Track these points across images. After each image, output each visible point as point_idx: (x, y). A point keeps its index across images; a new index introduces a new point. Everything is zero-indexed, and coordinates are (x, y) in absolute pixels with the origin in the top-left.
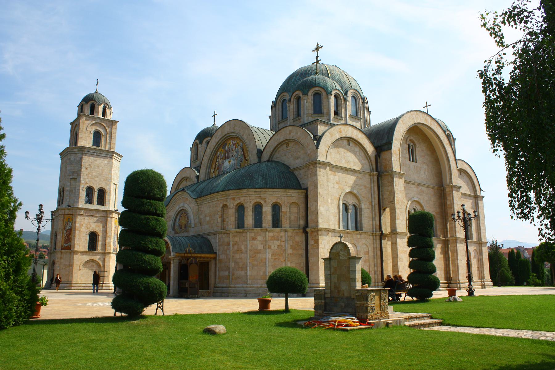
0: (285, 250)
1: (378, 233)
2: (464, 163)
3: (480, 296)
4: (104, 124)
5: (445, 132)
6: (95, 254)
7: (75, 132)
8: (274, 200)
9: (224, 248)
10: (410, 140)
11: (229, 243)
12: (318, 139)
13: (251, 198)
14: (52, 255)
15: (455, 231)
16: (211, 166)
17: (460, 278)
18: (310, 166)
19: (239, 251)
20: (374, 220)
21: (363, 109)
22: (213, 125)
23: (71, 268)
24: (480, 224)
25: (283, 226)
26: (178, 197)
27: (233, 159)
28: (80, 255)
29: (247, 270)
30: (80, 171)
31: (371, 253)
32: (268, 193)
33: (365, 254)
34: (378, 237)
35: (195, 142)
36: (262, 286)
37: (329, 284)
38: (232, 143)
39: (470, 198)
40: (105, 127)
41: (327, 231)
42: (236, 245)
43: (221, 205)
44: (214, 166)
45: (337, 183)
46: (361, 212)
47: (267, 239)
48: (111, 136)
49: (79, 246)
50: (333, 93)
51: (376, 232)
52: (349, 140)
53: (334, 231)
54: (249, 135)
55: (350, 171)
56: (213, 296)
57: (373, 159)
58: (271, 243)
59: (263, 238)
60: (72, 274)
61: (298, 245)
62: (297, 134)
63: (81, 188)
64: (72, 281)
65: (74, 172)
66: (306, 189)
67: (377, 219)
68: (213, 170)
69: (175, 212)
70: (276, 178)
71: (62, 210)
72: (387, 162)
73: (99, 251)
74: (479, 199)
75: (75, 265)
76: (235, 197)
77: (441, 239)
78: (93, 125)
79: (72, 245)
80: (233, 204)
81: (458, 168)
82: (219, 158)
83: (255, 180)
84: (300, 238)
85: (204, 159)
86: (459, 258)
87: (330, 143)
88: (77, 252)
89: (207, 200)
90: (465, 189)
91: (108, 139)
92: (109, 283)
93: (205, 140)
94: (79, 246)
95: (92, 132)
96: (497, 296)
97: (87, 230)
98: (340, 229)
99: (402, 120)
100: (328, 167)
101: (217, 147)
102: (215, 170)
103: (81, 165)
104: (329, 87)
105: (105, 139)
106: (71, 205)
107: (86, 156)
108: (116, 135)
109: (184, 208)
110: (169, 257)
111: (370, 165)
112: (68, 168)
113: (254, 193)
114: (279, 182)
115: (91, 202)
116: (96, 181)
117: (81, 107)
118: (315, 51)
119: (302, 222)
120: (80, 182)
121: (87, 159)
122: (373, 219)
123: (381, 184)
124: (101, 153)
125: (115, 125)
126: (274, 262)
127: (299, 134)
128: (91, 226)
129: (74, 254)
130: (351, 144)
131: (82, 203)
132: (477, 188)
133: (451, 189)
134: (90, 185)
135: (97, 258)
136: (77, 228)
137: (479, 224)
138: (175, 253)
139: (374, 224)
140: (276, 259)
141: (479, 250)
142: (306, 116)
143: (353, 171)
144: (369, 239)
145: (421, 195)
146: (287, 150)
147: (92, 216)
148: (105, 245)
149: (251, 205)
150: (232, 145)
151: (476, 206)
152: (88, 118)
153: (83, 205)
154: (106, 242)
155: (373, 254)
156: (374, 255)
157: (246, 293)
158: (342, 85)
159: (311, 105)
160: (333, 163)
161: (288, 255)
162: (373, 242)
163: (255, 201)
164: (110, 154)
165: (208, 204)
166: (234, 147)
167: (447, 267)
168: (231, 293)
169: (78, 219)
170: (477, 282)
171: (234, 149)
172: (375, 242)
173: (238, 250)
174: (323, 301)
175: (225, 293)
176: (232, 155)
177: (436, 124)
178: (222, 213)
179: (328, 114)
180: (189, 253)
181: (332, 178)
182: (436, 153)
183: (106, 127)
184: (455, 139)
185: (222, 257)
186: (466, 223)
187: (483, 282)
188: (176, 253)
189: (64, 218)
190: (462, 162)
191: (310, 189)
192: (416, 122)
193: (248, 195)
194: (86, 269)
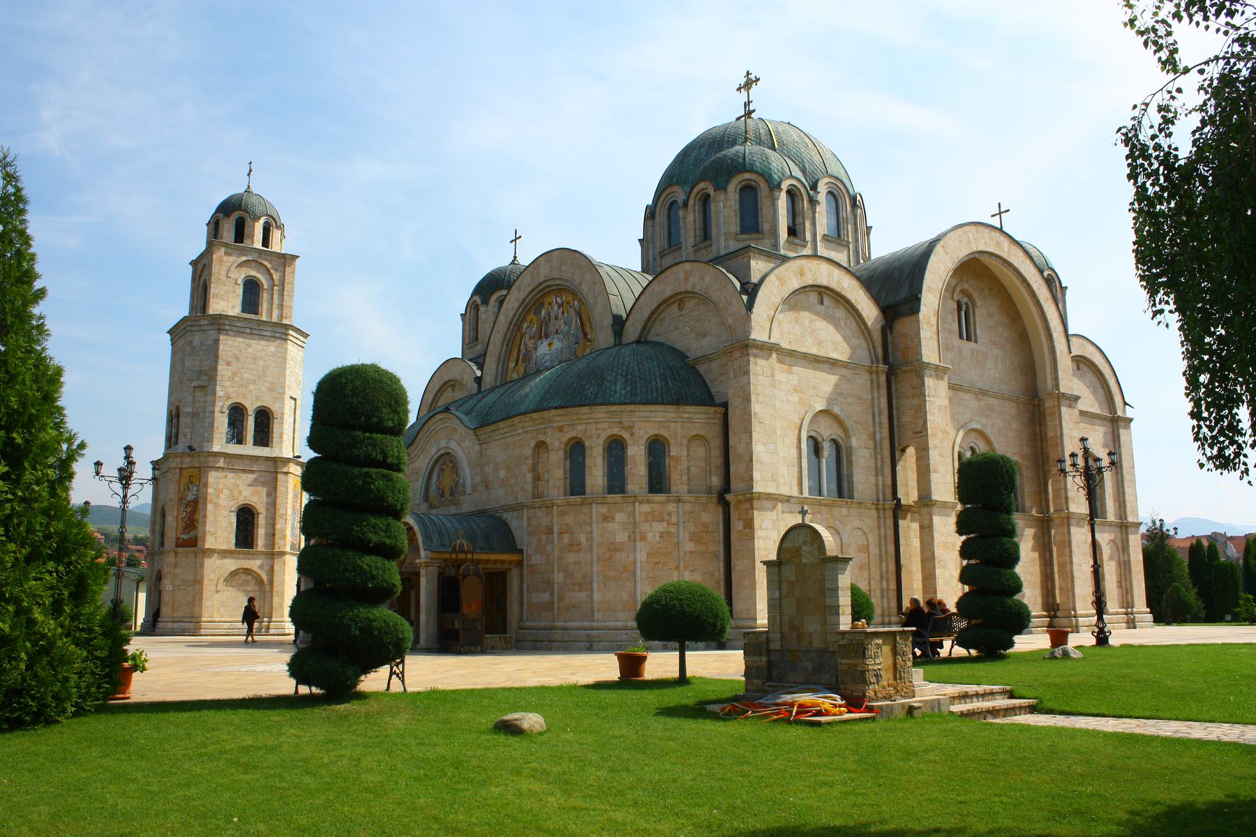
0: (678, 544)
1: (890, 504)
2: (1085, 342)
3: (1123, 646)
4: (266, 263)
5: (1041, 272)
6: (250, 556)
7: (201, 283)
8: (650, 430)
9: (540, 540)
10: (963, 291)
11: (552, 529)
12: (750, 290)
13: (599, 426)
14: (156, 558)
15: (1067, 498)
17: (1078, 605)
19: (574, 546)
20: (880, 474)
21: (852, 222)
22: (513, 262)
23: (197, 587)
24: (1122, 481)
25: (672, 488)
26: (434, 426)
28: (218, 558)
29: (592, 589)
30: (215, 369)
31: (874, 550)
32: (638, 413)
33: (859, 551)
34: (890, 514)
35: (471, 302)
36: (626, 626)
37: (778, 619)
38: (556, 302)
39: (1099, 422)
40: (268, 270)
41: (773, 499)
42: (566, 533)
43: (533, 444)
44: (515, 355)
45: (795, 391)
46: (849, 455)
47: (637, 520)
48: (283, 290)
49: (216, 538)
50: (785, 185)
51: (884, 500)
52: (822, 291)
53: (787, 499)
55: (824, 362)
56: (517, 649)
57: (877, 335)
58: (645, 527)
59: (629, 517)
60: (201, 600)
61: (707, 532)
62: (703, 280)
63: (217, 409)
64: (200, 617)
65: (200, 372)
66: (725, 405)
67: (888, 471)
68: (514, 364)
69: (428, 460)
70: (655, 380)
71: (177, 457)
72: (910, 343)
73: (259, 549)
74: (1121, 424)
75: (206, 582)
76: (562, 424)
77: (1033, 516)
78: (241, 265)
79: (199, 535)
80: (560, 440)
81: (1072, 355)
82: (527, 335)
83: (608, 385)
84: (712, 516)
85: (492, 338)
86: (1074, 559)
87: (778, 300)
88: (211, 552)
90: (1090, 402)
91: (276, 297)
92: (283, 622)
93: (494, 297)
94: (216, 538)
95: (240, 281)
96: (1161, 646)
97: (231, 503)
98: (802, 494)
99: (943, 246)
100: (774, 355)
103: (216, 356)
104: (776, 170)
105: (270, 297)
106: (195, 446)
107: (226, 335)
108: (293, 288)
109: (449, 451)
110: (417, 561)
111: (869, 349)
112: (188, 364)
113: (606, 415)
114: (664, 390)
115: (240, 441)
116: (251, 392)
117: (215, 227)
118: (742, 90)
119: (716, 481)
120: (215, 394)
121: (230, 343)
122: (878, 471)
123: (896, 390)
124: (261, 328)
125: (291, 264)
126: (653, 570)
127: (707, 279)
128: (240, 492)
129: (203, 557)
130: (826, 300)
131: (219, 443)
132: (1118, 399)
133: (1056, 403)
134: (238, 401)
135: (255, 564)
136: (209, 498)
137: (1120, 482)
138: (429, 552)
139: (880, 483)
140: (659, 562)
141: (1122, 541)
142: (723, 237)
143: (832, 364)
144: (869, 517)
145: (986, 416)
146: (681, 315)
147: (244, 471)
148: (274, 535)
149: (601, 442)
150: (556, 307)
151: (1114, 441)
152: (229, 251)
153: (222, 447)
154: (274, 530)
155: (877, 552)
156: (880, 555)
157: (590, 642)
158: (804, 166)
159: (733, 214)
160: (785, 345)
161: (685, 553)
162: (879, 523)
163: (609, 433)
164: (281, 331)
165: (502, 441)
166: (561, 311)
167: (1047, 581)
168: (557, 641)
169: (213, 477)
170: (1117, 614)
171: (560, 315)
172: (882, 525)
173: (573, 545)
174: (764, 659)
175: (542, 641)
176: (557, 331)
177: (1021, 254)
178: (534, 460)
179: (773, 234)
180: (462, 550)
181: (782, 380)
182: (1022, 320)
183: (272, 271)
184: (1066, 288)
185: (537, 559)
186: (1092, 479)
187: (1132, 614)
188: (432, 551)
189: (181, 476)
190: (1081, 341)
191: (734, 404)
192: (975, 249)
193: (592, 420)
194: (231, 589)
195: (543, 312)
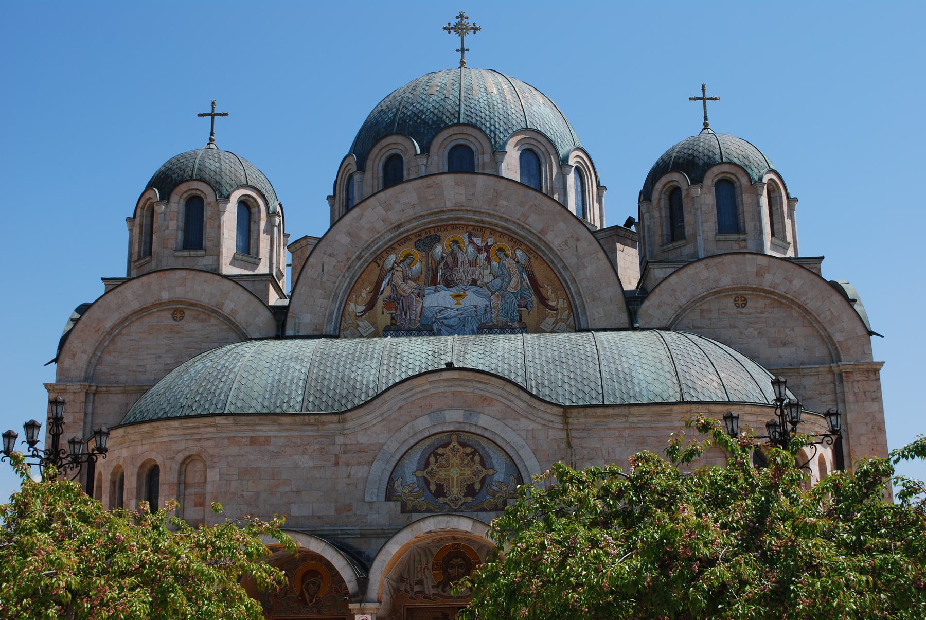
16: (352, 290)
18: (852, 372)
27: (475, 292)
38: (471, 242)
44: (365, 294)
54: (578, 240)
62: (791, 282)
68: (363, 308)
82: (398, 274)
89: (631, 419)
101: (390, 240)
102: (371, 305)
127: (797, 283)
146: (741, 313)
150: (471, 249)
165: (627, 431)
195: (439, 250)
